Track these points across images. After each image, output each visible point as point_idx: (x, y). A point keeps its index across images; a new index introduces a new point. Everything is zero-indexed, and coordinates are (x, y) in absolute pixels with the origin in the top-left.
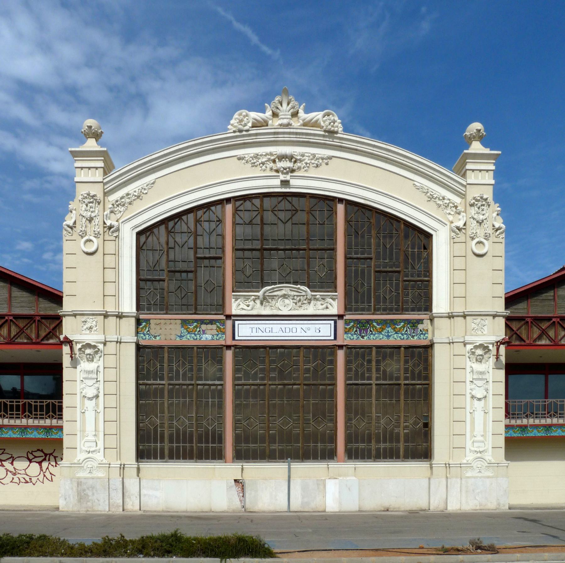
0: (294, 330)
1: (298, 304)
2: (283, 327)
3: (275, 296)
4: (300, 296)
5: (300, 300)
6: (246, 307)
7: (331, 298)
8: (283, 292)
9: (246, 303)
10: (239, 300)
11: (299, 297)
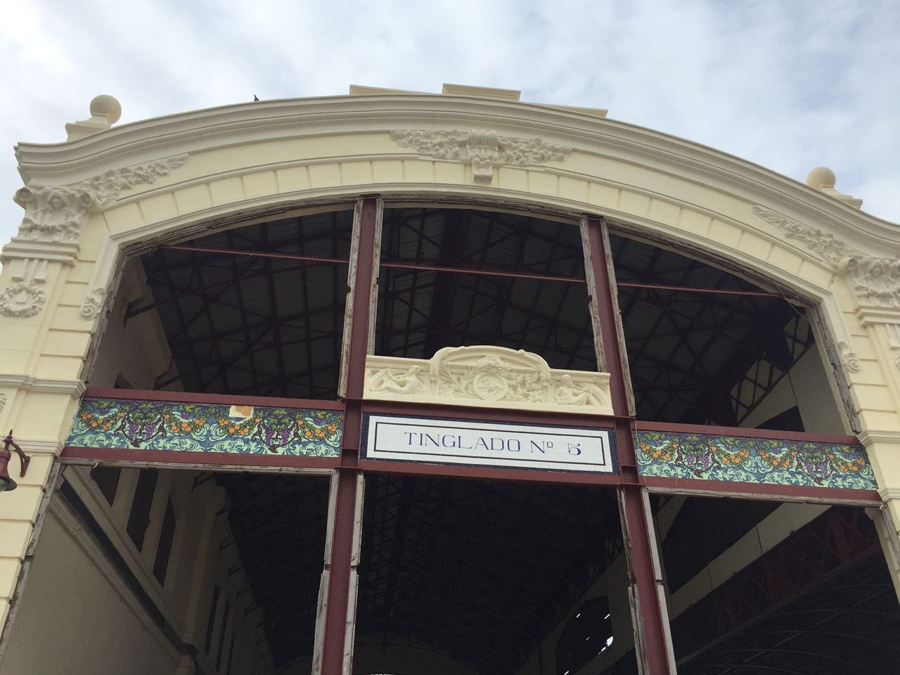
0: (514, 446)
1: (519, 389)
2: (487, 436)
3: (467, 368)
4: (525, 372)
5: (523, 384)
6: (397, 387)
7: (595, 383)
9: (399, 378)
10: (381, 373)
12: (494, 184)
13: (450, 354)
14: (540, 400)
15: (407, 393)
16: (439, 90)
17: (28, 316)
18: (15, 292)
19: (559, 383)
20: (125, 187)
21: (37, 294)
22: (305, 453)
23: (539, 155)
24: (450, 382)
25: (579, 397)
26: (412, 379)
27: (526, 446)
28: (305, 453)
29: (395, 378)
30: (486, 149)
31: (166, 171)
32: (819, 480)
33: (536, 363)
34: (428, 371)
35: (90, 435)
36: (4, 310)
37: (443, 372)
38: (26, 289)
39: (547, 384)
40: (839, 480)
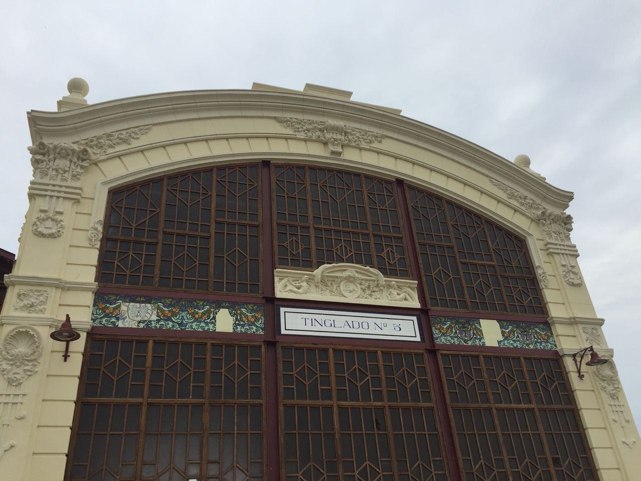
0: (365, 326)
1: (367, 291)
2: (350, 319)
3: (337, 277)
4: (370, 280)
5: (369, 287)
6: (295, 289)
7: (409, 287)
8: (345, 274)
9: (296, 283)
10: (285, 280)
11: (368, 282)
12: (342, 157)
13: (327, 269)
14: (379, 298)
15: (303, 294)
16: (300, 88)
17: (55, 238)
18: (43, 220)
19: (389, 286)
20: (111, 146)
21: (59, 222)
22: (158, 327)
23: (368, 140)
24: (327, 285)
25: (401, 296)
26: (304, 284)
27: (372, 325)
28: (158, 327)
29: (293, 283)
30: (336, 133)
31: (138, 136)
32: (528, 345)
33: (376, 275)
34: (313, 279)
35: (196, 323)
36: (37, 233)
37: (323, 281)
38: (51, 218)
39: (382, 288)
40: (538, 344)
